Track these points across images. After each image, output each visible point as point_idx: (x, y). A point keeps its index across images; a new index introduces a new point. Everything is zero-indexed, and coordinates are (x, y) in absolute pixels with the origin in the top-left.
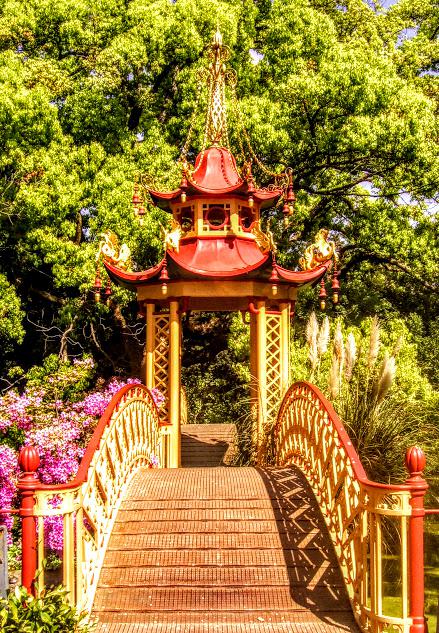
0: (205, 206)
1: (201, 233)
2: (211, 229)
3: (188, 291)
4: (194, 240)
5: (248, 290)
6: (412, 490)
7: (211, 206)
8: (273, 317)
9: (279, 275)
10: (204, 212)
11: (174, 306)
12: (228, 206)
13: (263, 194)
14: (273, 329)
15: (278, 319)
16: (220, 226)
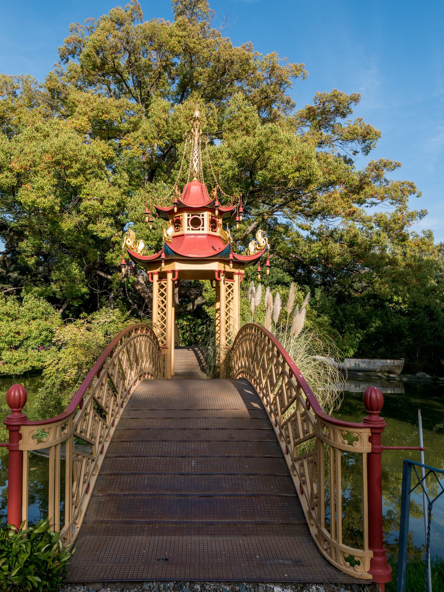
0: (189, 216)
1: (186, 232)
2: (192, 230)
3: (179, 266)
4: (183, 235)
5: (214, 266)
6: (372, 428)
7: (192, 215)
8: (230, 283)
9: (234, 257)
10: (188, 219)
11: (170, 276)
12: (203, 215)
13: (223, 209)
14: (230, 291)
15: (232, 284)
16: (197, 228)
